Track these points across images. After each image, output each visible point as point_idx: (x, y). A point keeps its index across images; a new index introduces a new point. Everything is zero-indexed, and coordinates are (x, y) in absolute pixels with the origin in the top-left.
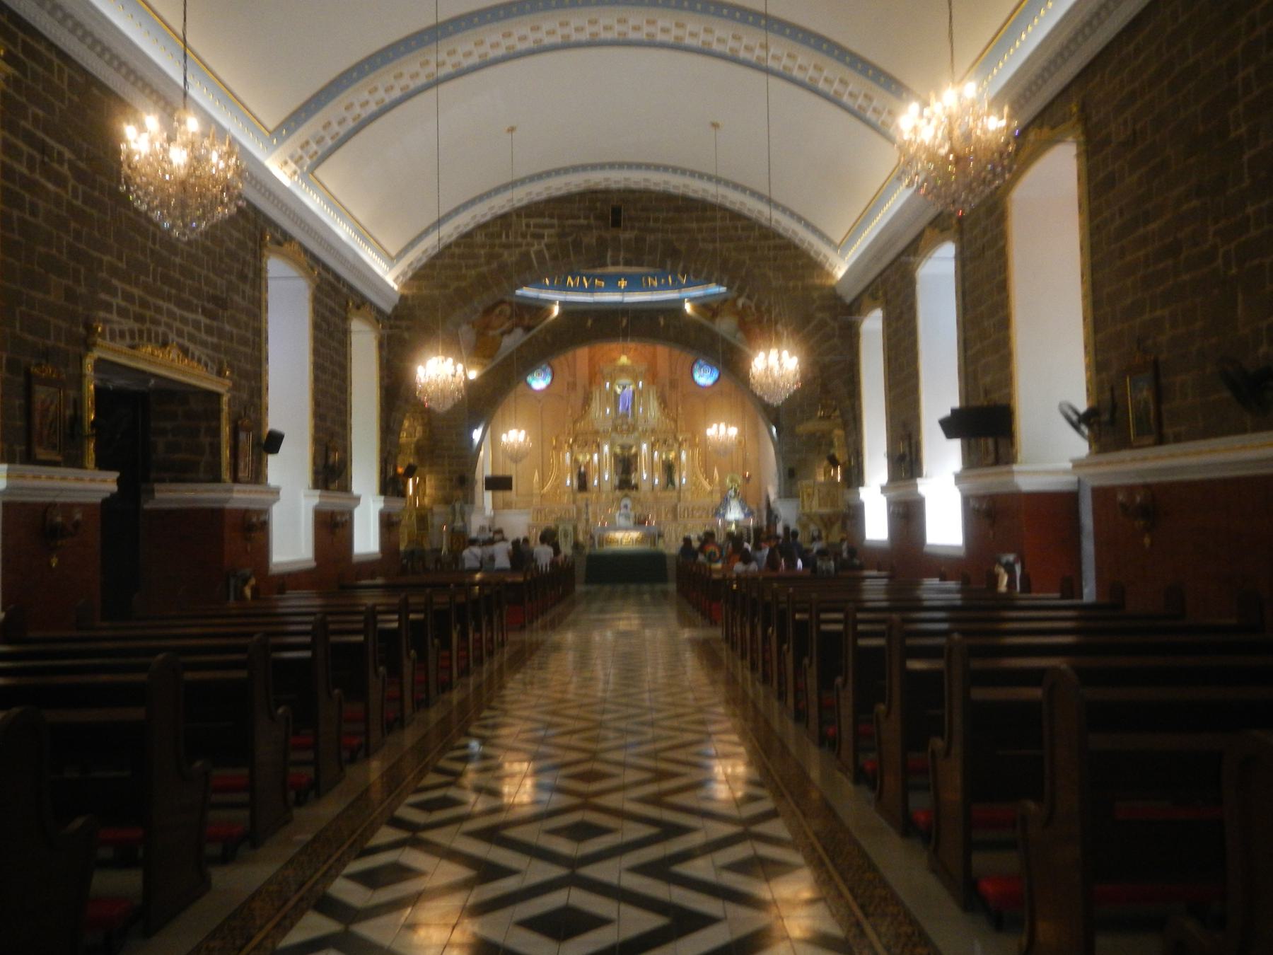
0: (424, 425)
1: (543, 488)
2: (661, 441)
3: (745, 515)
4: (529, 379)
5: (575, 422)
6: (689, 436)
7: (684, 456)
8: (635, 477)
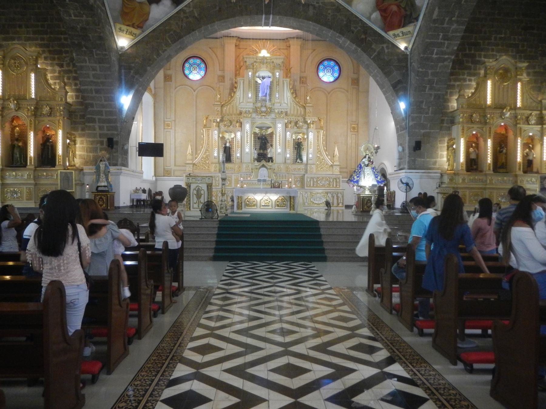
0: (78, 90)
1: (196, 158)
2: (293, 124)
3: (378, 182)
4: (187, 72)
5: (222, 106)
6: (316, 120)
7: (311, 136)
8: (271, 150)
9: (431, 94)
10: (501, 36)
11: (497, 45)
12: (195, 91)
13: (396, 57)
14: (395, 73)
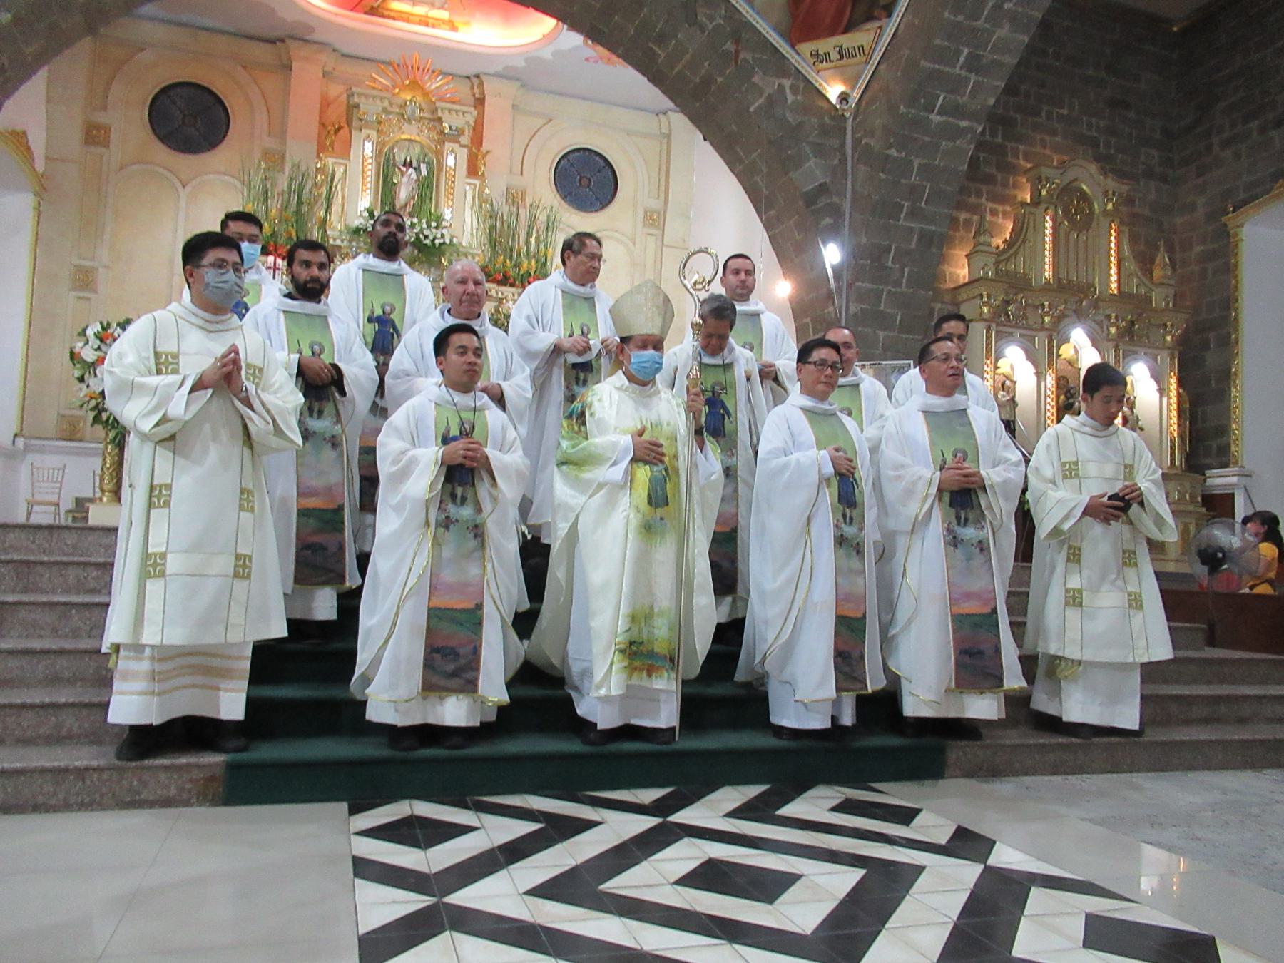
9: (912, 229)
10: (1061, 111)
11: (1054, 133)
12: (184, 187)
13: (814, 120)
14: (811, 161)
